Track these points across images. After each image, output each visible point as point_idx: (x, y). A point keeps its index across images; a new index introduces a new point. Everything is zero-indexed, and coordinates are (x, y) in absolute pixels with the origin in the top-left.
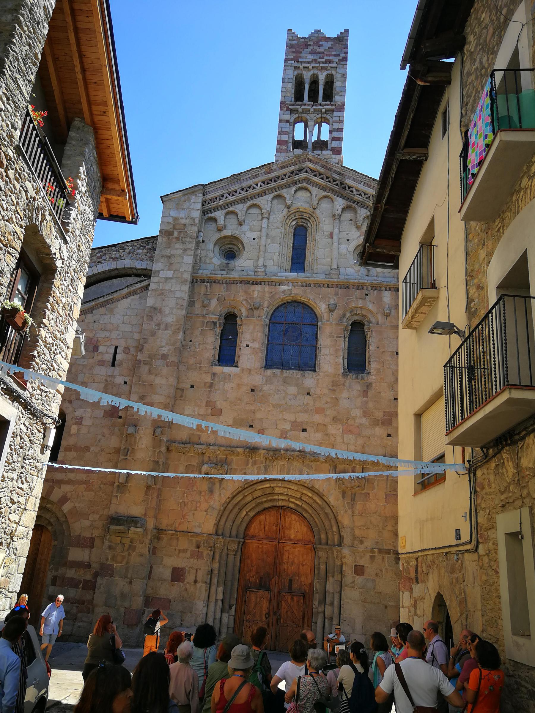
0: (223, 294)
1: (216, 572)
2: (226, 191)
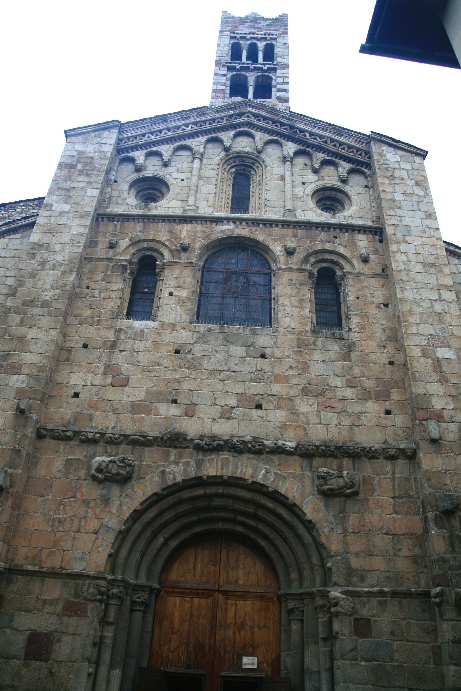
0: (138, 233)
1: (109, 641)
2: (149, 131)
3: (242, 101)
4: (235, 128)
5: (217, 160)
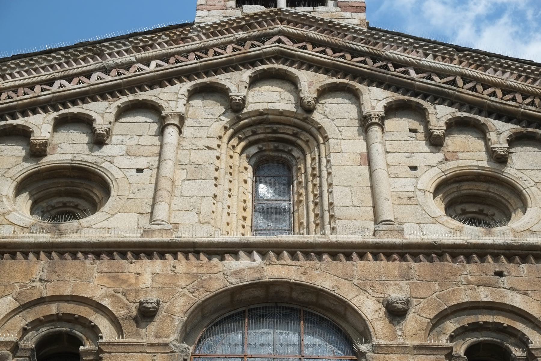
3: (264, 13)
4: (253, 65)
5: (216, 128)
